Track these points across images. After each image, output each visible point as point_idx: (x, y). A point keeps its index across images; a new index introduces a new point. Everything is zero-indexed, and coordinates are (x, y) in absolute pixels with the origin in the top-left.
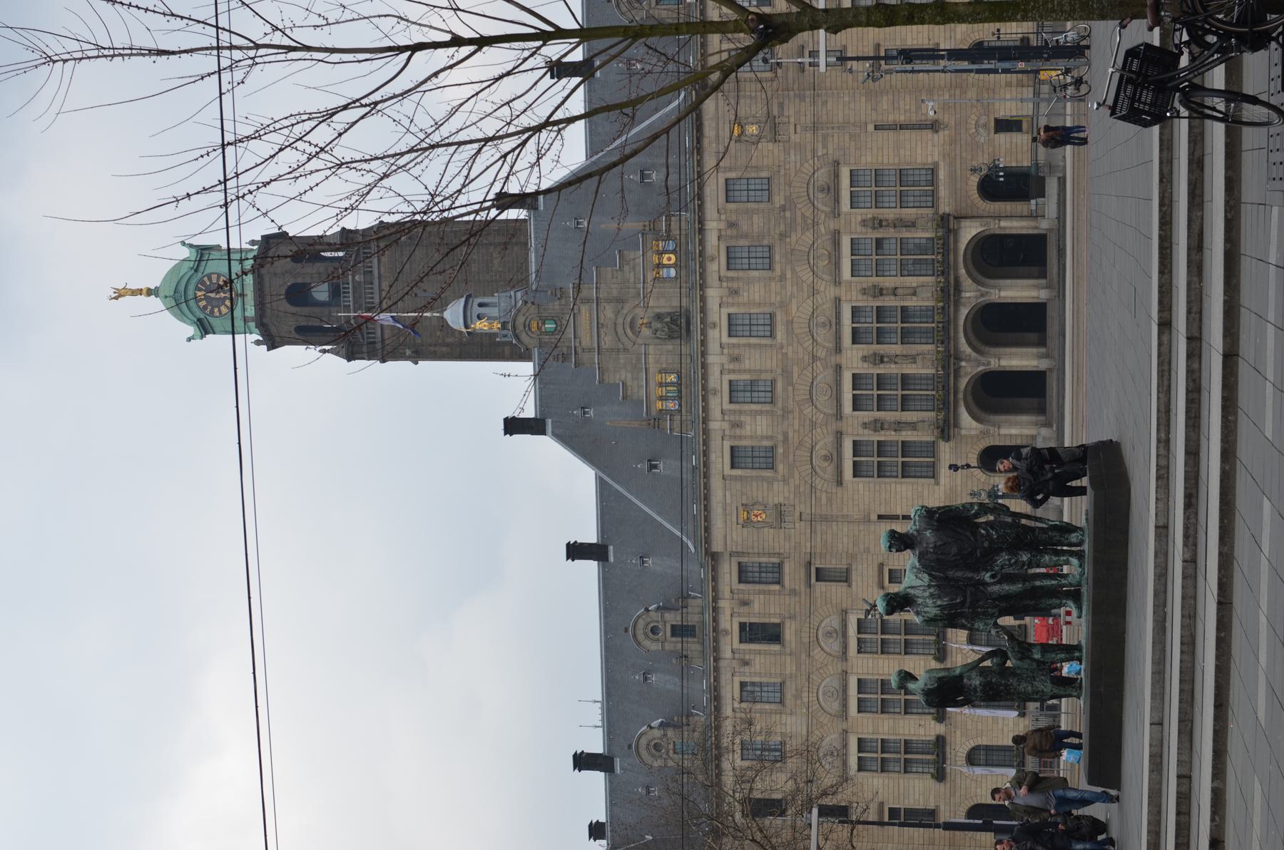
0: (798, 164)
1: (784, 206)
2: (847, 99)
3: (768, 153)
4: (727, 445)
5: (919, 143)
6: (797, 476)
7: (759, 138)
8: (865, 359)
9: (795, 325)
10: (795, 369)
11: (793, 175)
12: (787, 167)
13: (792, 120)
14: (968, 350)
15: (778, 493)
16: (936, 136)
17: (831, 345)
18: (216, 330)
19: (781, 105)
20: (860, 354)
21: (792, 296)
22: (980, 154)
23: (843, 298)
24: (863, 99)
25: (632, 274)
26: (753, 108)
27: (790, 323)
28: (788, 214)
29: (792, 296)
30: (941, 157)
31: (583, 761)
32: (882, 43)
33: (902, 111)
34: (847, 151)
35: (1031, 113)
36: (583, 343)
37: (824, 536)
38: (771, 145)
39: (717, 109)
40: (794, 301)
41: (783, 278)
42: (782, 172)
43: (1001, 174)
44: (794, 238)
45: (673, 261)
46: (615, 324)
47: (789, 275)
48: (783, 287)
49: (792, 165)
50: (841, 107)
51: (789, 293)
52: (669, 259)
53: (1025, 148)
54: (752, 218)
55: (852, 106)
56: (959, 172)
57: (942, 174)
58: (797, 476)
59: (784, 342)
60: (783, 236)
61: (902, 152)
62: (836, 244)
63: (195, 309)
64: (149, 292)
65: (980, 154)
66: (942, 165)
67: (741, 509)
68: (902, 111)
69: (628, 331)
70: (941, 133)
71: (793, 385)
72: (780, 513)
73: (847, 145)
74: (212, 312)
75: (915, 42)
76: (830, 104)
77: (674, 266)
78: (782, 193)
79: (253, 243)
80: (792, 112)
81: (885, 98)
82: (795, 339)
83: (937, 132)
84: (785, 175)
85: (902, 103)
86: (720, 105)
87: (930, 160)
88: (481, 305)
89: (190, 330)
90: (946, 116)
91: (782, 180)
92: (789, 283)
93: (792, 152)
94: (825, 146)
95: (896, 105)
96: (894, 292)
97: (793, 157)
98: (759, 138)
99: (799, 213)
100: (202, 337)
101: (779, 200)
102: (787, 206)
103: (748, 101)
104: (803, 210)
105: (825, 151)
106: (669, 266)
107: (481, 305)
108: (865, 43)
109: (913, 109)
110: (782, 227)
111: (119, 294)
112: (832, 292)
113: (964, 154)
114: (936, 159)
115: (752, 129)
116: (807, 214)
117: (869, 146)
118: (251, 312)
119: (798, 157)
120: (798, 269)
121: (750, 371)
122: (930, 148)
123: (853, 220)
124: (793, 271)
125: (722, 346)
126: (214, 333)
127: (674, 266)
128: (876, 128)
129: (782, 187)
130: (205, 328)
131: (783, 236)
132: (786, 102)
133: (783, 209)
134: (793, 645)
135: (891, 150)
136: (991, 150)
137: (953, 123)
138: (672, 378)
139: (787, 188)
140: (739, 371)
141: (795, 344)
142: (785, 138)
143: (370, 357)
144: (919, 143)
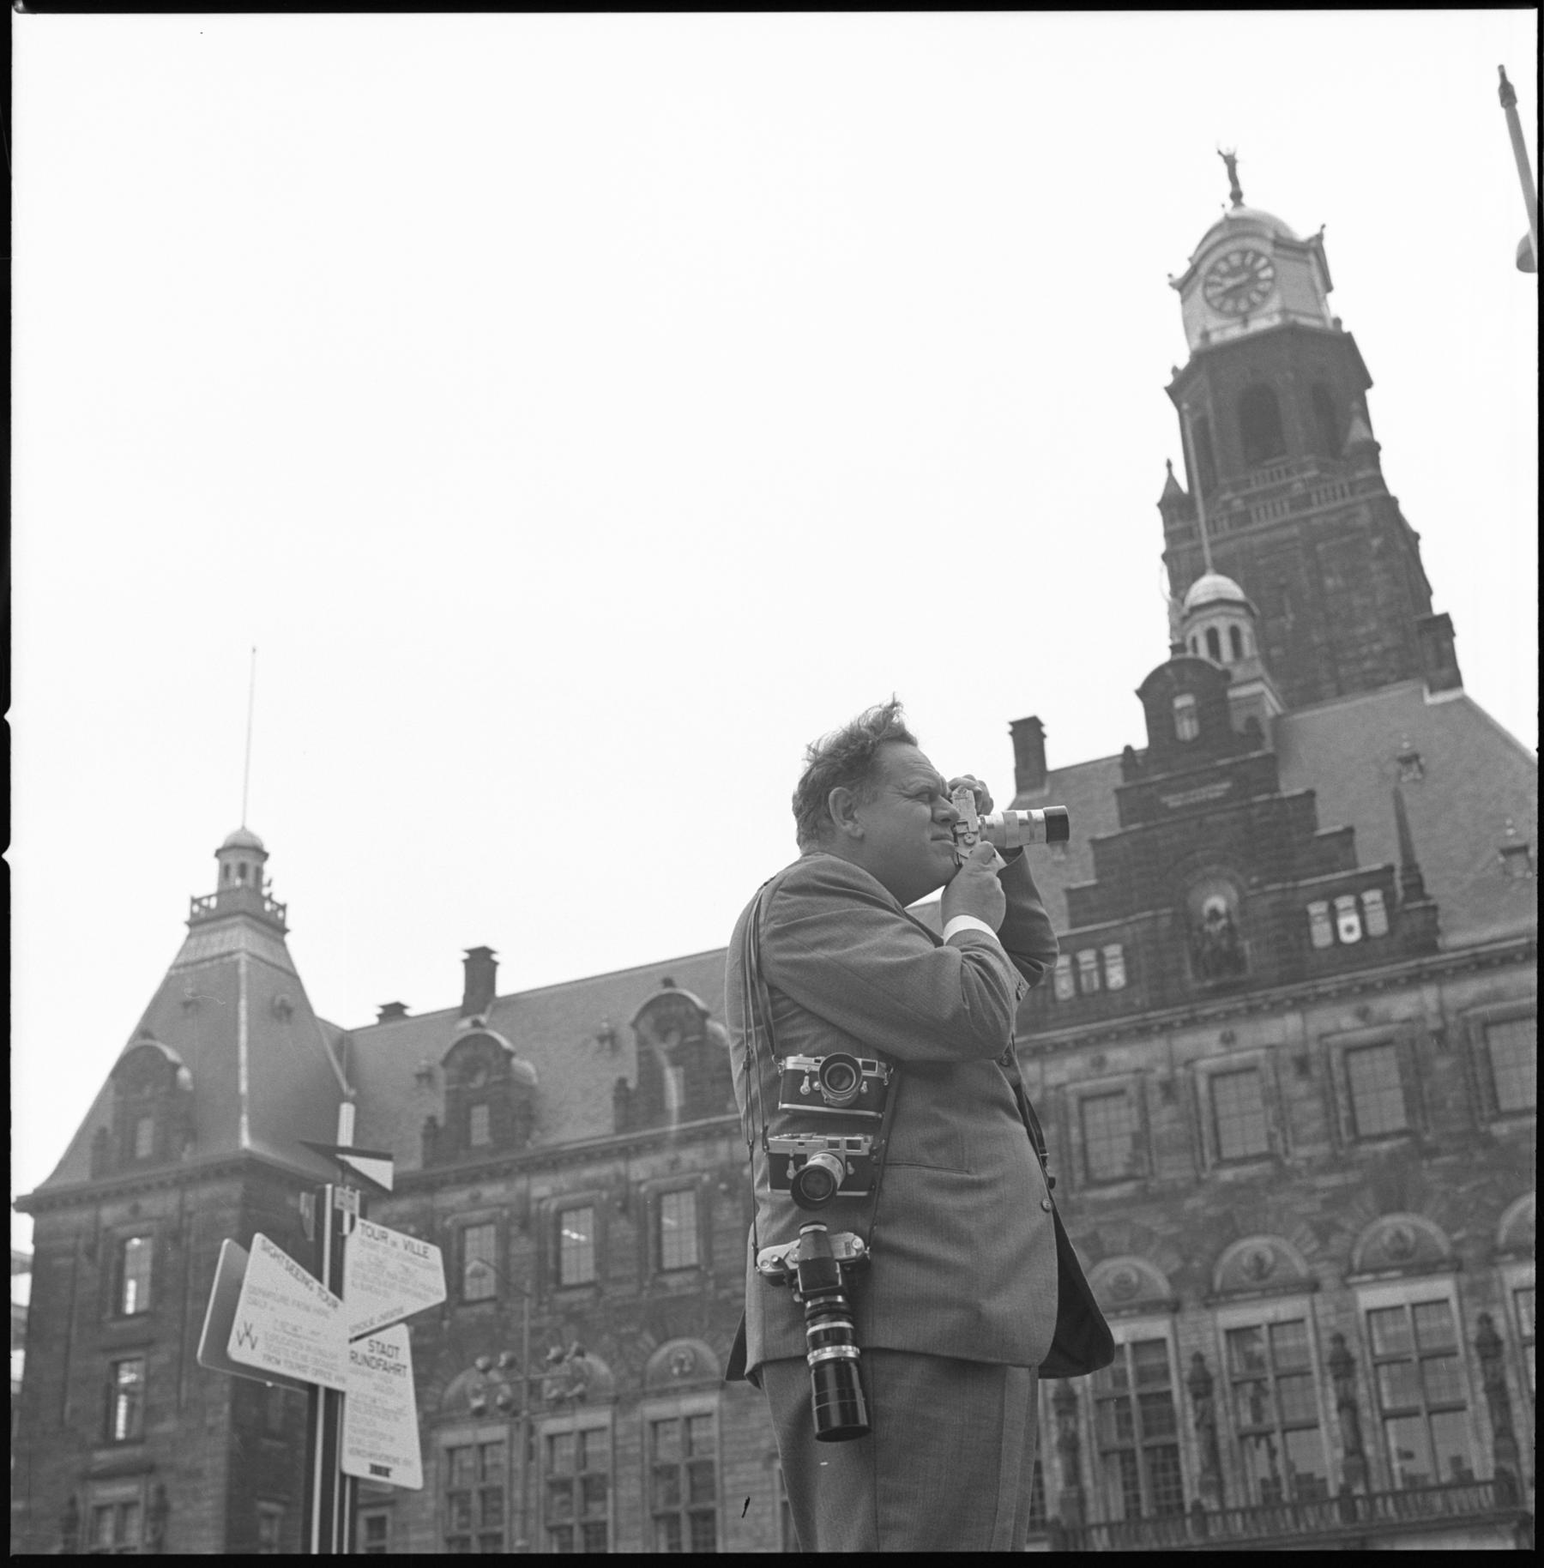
18: (1187, 303)
31: (480, 964)
45: (1347, 938)
48: (1325, 1170)
52: (1350, 929)
64: (1237, 196)
74: (1213, 284)
79: (1338, 322)
88: (1235, 633)
89: (1181, 269)
92: (1334, 1180)
100: (1173, 285)
107: (1235, 633)
111: (1231, 162)
118: (1216, 338)
125: (1189, 1063)
126: (1183, 301)
130: (1183, 286)
143: (1169, 535)
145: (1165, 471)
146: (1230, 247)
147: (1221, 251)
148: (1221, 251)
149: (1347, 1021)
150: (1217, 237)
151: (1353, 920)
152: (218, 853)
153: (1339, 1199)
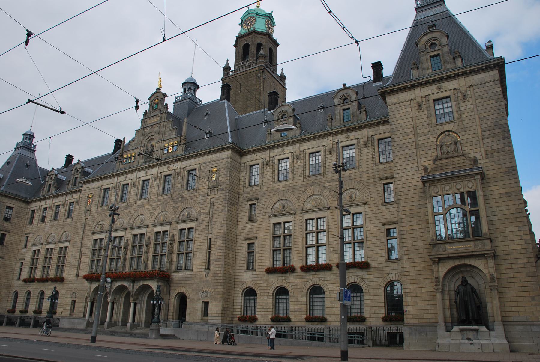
0: (198, 202)
1: (183, 197)
2: (223, 222)
3: (204, 186)
4: (110, 186)
5: (201, 261)
6: (98, 216)
7: (210, 180)
8: (127, 240)
9: (142, 208)
10: (128, 211)
11: (194, 199)
12: (198, 197)
13: (216, 196)
14: (114, 288)
15: (94, 208)
16: (203, 270)
17: (134, 225)
19: (222, 190)
20: (129, 239)
21: (152, 205)
22: (194, 293)
23: (148, 229)
24: (222, 231)
25: (167, 135)
26: (223, 176)
27: (142, 206)
28: (180, 199)
29: (152, 205)
30: (195, 273)
32: (257, 241)
33: (215, 252)
34: (201, 225)
35: (209, 321)
36: (148, 121)
37: (80, 229)
38: (207, 187)
39: (223, 159)
40: (150, 207)
41: (158, 200)
42: (196, 194)
43: (155, 302)
44: (171, 203)
46: (152, 132)
47: (159, 203)
49: (198, 199)
50: (219, 220)
51: (152, 204)
53: (195, 318)
54: (180, 183)
55: (219, 225)
56: (188, 282)
57: (188, 273)
58: (98, 216)
59: (137, 204)
60: (172, 198)
61: (198, 253)
62: (165, 224)
63: (245, 18)
65: (194, 293)
66: (192, 273)
67: (92, 194)
68: (215, 252)
69: (150, 138)
70: (204, 273)
71: (124, 210)
72: (88, 211)
73: (203, 225)
75: (257, 258)
76: (221, 214)
77: (168, 152)
78: (188, 195)
80: (219, 195)
81: (221, 242)
82: (138, 209)
83: (205, 270)
84: (195, 196)
85: (219, 251)
86: (225, 160)
87: (194, 267)
90: (211, 275)
91: (193, 195)
93: (203, 198)
94: (204, 213)
95: (218, 248)
96: (147, 253)
97: (201, 198)
98: (210, 180)
99: (179, 204)
101: (185, 194)
102: (183, 199)
103: (226, 173)
104: (181, 206)
105: (202, 214)
106: (168, 150)
108: (258, 232)
109: (216, 257)
110: (176, 198)
112: (151, 223)
113: (195, 285)
114: (194, 270)
115: (214, 177)
116: (179, 209)
117: (203, 236)
119: (201, 201)
120: (160, 207)
121: (131, 191)
122: (199, 267)
123: (175, 230)
124: (160, 205)
127: (168, 152)
128: (211, 239)
129: (190, 195)
131: (172, 198)
132: (224, 192)
133: (182, 197)
134: (65, 223)
135: (199, 247)
136: (196, 299)
137: (208, 278)
138: (133, 160)
139: (190, 197)
140: (131, 187)
141: (136, 209)
142: (209, 193)
144: (201, 261)
145: (226, 62)
146: (249, 16)
147: (247, 17)
148: (247, 17)
149: (165, 170)
150: (247, 14)
151: (172, 148)
152: (24, 134)
153: (156, 208)
